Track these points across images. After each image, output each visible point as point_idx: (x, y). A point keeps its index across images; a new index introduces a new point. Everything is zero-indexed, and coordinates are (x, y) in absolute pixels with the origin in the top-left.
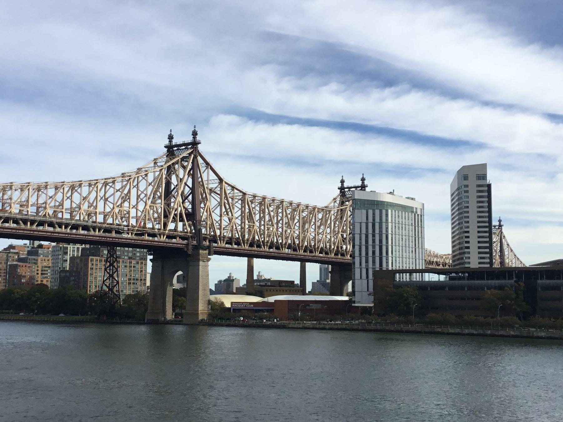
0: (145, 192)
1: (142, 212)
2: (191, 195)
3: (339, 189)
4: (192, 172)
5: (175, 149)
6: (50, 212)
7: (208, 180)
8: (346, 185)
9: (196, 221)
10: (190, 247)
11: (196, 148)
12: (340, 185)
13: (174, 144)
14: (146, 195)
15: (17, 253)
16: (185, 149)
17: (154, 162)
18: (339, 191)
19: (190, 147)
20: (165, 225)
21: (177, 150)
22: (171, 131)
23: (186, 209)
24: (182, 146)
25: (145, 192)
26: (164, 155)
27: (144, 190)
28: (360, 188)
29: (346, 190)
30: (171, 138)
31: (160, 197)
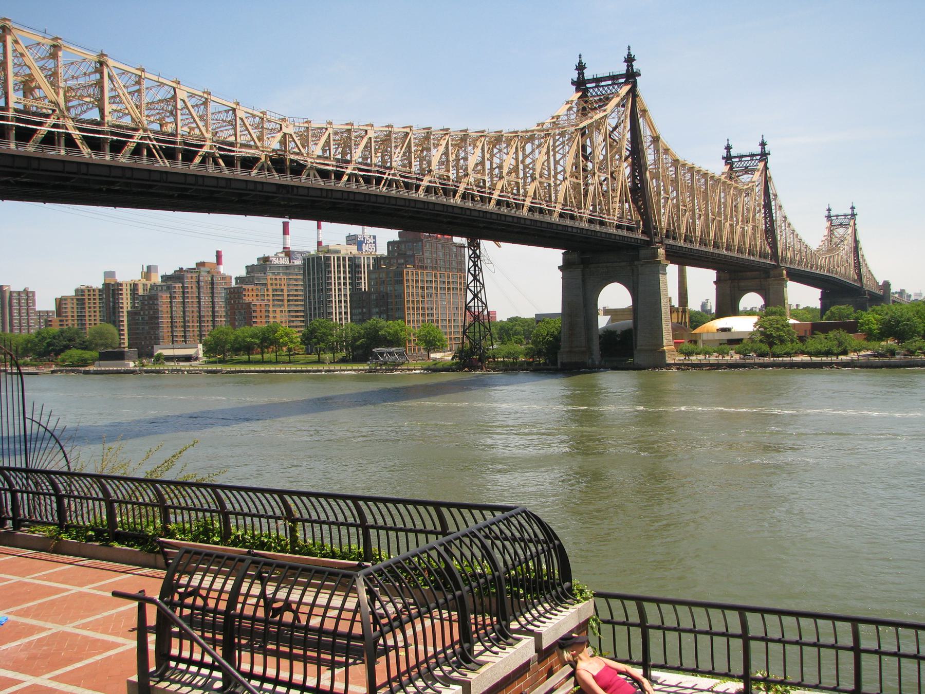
3: (723, 158)
5: (594, 85)
8: (733, 152)
12: (724, 153)
15: (209, 272)
17: (569, 106)
18: (724, 161)
19: (622, 80)
21: (596, 87)
22: (580, 57)
24: (602, 81)
28: (758, 157)
29: (734, 160)
30: (581, 68)
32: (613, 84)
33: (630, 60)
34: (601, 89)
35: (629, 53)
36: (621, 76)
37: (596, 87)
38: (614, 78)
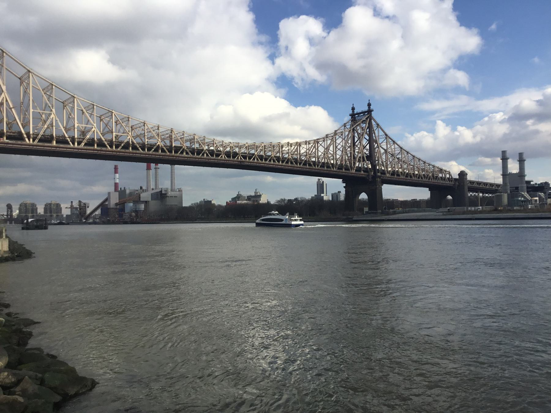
0: (341, 144)
1: (340, 156)
2: (368, 144)
4: (368, 130)
6: (308, 157)
7: (378, 136)
9: (373, 161)
10: (370, 177)
11: (371, 115)
13: (355, 112)
14: (342, 146)
16: (363, 115)
19: (366, 113)
20: (354, 163)
23: (365, 153)
25: (341, 144)
26: (349, 121)
27: (340, 143)
31: (349, 147)
33: (369, 105)
36: (365, 112)
38: (364, 113)
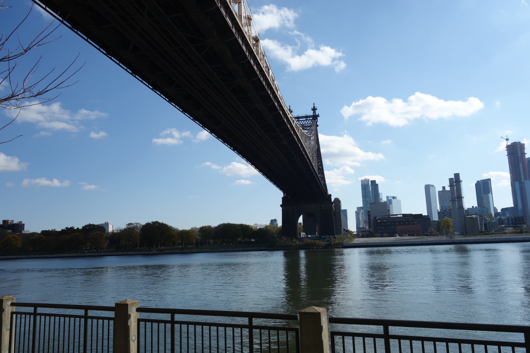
19: (311, 118)
32: (307, 120)
33: (314, 109)
34: (300, 122)
35: (314, 106)
37: (298, 121)
38: (306, 117)
